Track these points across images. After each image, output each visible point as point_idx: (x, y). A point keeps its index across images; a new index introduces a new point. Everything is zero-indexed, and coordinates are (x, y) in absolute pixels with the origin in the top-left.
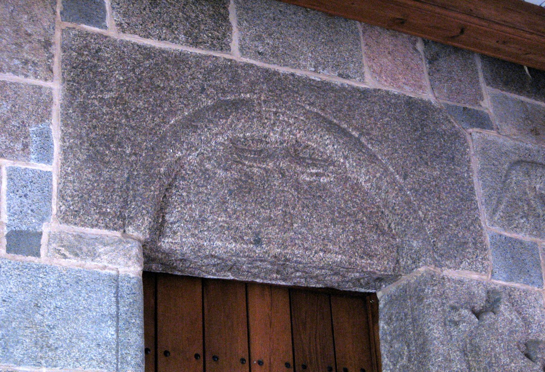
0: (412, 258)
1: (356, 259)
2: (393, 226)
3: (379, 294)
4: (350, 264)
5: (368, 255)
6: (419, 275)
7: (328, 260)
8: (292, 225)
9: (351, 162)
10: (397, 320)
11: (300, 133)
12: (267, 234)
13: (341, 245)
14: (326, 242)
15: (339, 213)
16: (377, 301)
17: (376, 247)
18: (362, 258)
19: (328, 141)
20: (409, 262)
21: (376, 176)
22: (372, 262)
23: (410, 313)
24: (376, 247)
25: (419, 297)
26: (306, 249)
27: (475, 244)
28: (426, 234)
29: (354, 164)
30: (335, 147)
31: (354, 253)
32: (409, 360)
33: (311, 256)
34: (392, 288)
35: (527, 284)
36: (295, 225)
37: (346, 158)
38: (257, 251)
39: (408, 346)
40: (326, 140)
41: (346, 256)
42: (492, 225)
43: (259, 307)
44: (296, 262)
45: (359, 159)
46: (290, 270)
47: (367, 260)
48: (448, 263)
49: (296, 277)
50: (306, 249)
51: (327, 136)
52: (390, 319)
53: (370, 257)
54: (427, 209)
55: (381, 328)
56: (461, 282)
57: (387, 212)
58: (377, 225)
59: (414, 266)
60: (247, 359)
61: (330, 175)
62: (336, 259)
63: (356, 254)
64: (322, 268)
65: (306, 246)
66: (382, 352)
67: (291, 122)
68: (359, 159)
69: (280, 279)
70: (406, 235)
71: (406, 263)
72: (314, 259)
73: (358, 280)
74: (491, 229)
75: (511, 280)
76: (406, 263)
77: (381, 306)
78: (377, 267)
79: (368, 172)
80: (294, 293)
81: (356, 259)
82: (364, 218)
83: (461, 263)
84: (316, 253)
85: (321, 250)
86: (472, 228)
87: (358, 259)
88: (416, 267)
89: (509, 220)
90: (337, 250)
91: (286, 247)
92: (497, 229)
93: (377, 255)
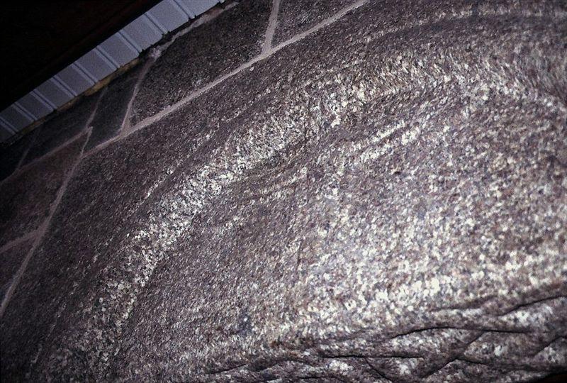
1: (486, 271)
7: (403, 303)
9: (459, 67)
11: (359, 88)
13: (435, 253)
17: (550, 212)
19: (405, 64)
21: (514, 54)
22: (541, 258)
24: (550, 212)
26: (341, 299)
29: (466, 66)
30: (420, 64)
31: (476, 257)
33: (360, 310)
37: (447, 68)
40: (400, 66)
41: (449, 274)
45: (470, 50)
47: (522, 259)
51: (400, 58)
61: (420, 120)
62: (426, 293)
63: (482, 257)
65: (337, 293)
67: (339, 82)
68: (470, 50)
79: (495, 58)
81: (486, 271)
82: (510, 161)
87: (491, 266)
93: (550, 234)
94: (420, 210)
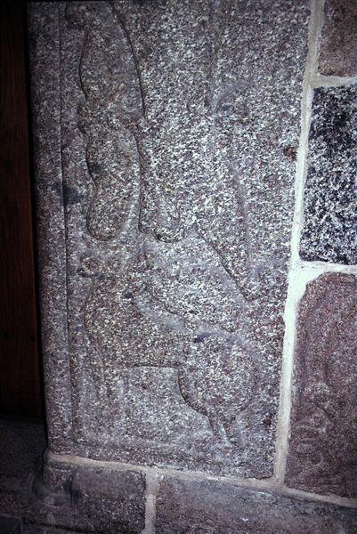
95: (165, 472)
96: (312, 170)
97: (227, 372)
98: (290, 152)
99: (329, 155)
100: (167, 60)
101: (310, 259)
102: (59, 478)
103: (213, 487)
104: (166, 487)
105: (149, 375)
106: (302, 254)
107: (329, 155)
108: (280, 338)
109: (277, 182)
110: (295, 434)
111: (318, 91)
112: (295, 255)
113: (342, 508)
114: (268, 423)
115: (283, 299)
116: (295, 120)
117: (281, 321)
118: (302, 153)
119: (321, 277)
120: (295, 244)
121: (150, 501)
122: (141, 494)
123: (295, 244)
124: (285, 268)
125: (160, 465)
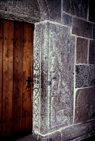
0: (44, 18)
2: (41, 8)
3: (35, 24)
4: (29, 18)
5: (34, 16)
6: (45, 22)
8: (15, 6)
10: (38, 31)
12: (9, 8)
14: (24, 11)
15: (28, 4)
16: (34, 26)
18: (32, 16)
20: (43, 19)
23: (41, 31)
25: (44, 27)
26: (19, 13)
27: (59, 15)
28: (48, 12)
32: (40, 42)
34: (38, 23)
35: (68, 26)
36: (16, 6)
38: (6, 12)
39: (40, 38)
42: (64, 11)
43: (6, 25)
44: (16, 16)
46: (14, 17)
48: (52, 20)
49: (15, 19)
50: (19, 13)
52: (37, 30)
53: (34, 16)
54: (49, 5)
55: (34, 32)
56: (54, 25)
57: (40, 5)
58: (37, 8)
59: (44, 20)
60: (2, 37)
64: (22, 18)
66: (34, 38)
69: (11, 19)
70: (44, 11)
71: (42, 18)
72: (20, 16)
73: (31, 21)
74: (63, 12)
75: (65, 25)
76: (42, 18)
77: (35, 27)
78: (35, 19)
80: (15, 22)
83: (55, 20)
84: (21, 14)
85: (22, 14)
86: (59, 11)
88: (45, 20)
89: (67, 11)
90: (26, 14)
91: (13, 12)
92: (64, 12)
94: (26, 6)
95: (61, 129)
96: (76, 76)
97: (70, 107)
98: (74, 73)
99: (77, 74)
100: (64, 62)
101: (76, 88)
102: (46, 139)
103: (67, 128)
104: (62, 131)
105: (59, 112)
106: (75, 87)
107: (77, 74)
108: (73, 100)
109: (73, 78)
110: (75, 115)
111: (76, 65)
112: (74, 88)
113: (80, 124)
114: (72, 114)
115: (73, 94)
116: (74, 69)
117: (73, 98)
118: (75, 73)
119: (77, 90)
120: (75, 86)
121: (62, 135)
122: (60, 134)
123: (75, 86)
124: (73, 90)
125: (60, 128)
